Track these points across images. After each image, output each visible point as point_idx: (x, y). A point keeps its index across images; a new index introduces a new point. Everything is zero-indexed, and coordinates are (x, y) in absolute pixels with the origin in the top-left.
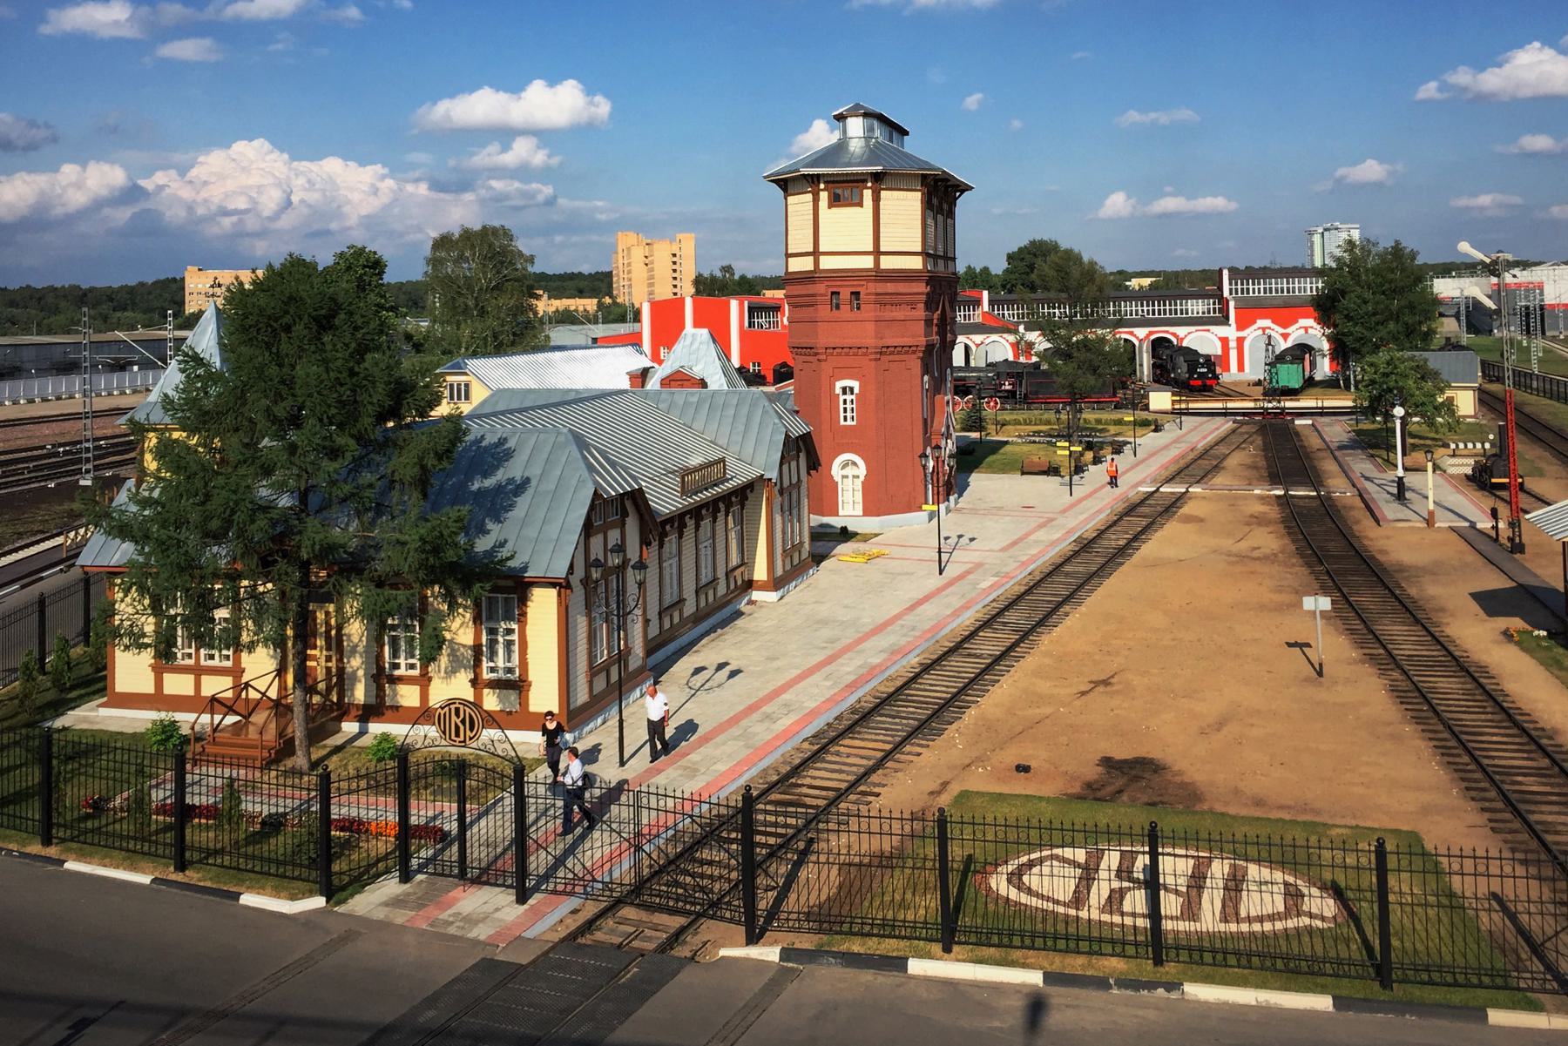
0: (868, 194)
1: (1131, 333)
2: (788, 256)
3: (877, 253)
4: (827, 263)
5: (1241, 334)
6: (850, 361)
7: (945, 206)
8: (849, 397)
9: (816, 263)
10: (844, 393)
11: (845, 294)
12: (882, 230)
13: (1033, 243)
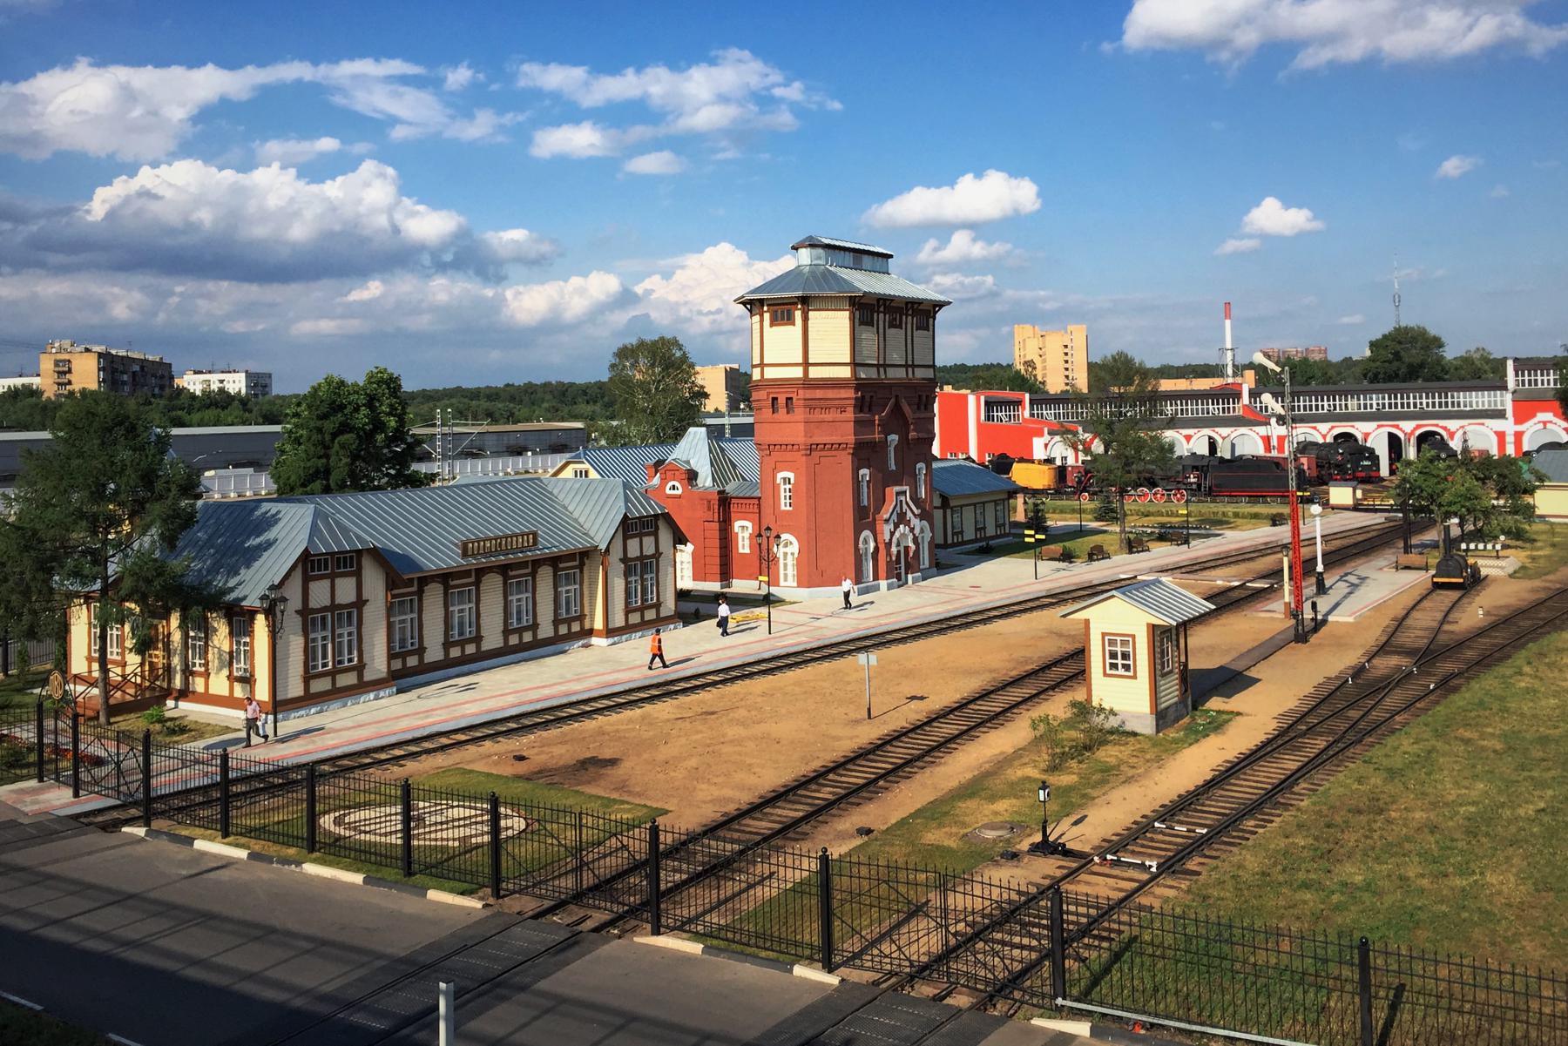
0: (798, 314)
1: (1397, 427)
3: (806, 364)
5: (1520, 428)
6: (788, 456)
11: (782, 401)
13: (1397, 330)
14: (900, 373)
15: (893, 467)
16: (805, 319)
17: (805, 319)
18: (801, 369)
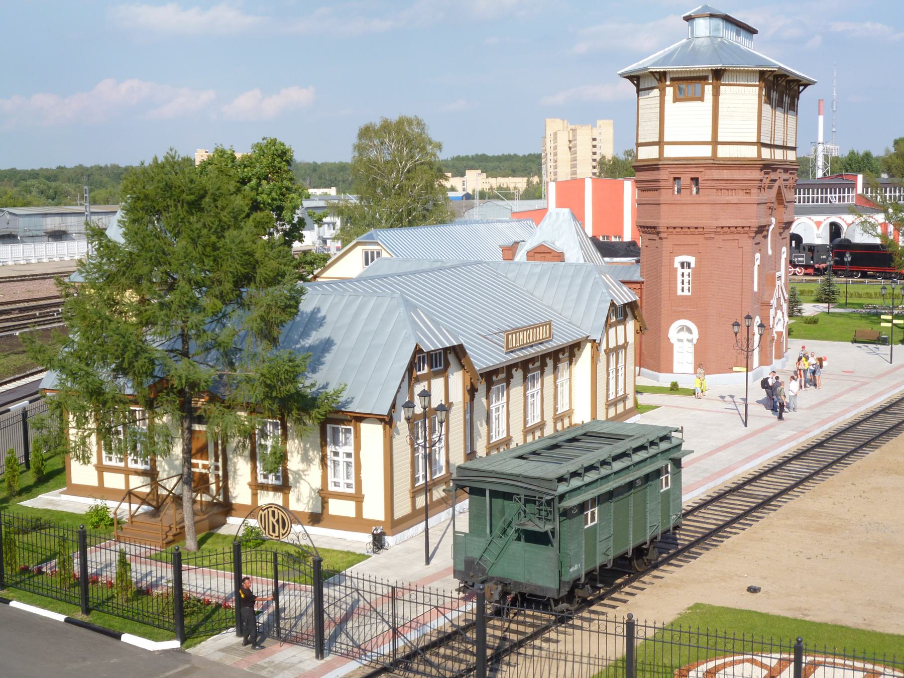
2: (639, 145)
4: (670, 152)
6: (689, 239)
7: (787, 100)
8: (686, 271)
9: (661, 152)
10: (683, 267)
12: (720, 122)
14: (779, 155)
15: (770, 252)
16: (716, 94)
17: (716, 94)
18: (710, 147)
